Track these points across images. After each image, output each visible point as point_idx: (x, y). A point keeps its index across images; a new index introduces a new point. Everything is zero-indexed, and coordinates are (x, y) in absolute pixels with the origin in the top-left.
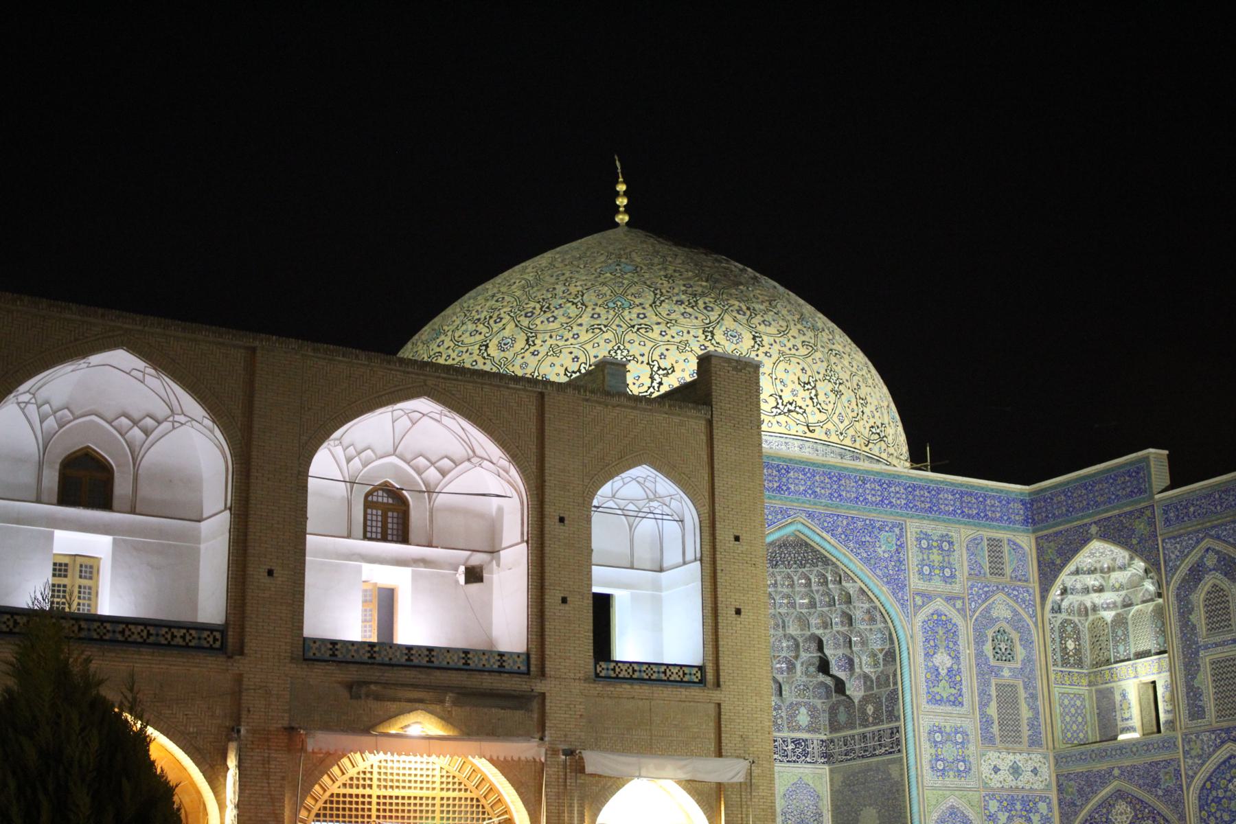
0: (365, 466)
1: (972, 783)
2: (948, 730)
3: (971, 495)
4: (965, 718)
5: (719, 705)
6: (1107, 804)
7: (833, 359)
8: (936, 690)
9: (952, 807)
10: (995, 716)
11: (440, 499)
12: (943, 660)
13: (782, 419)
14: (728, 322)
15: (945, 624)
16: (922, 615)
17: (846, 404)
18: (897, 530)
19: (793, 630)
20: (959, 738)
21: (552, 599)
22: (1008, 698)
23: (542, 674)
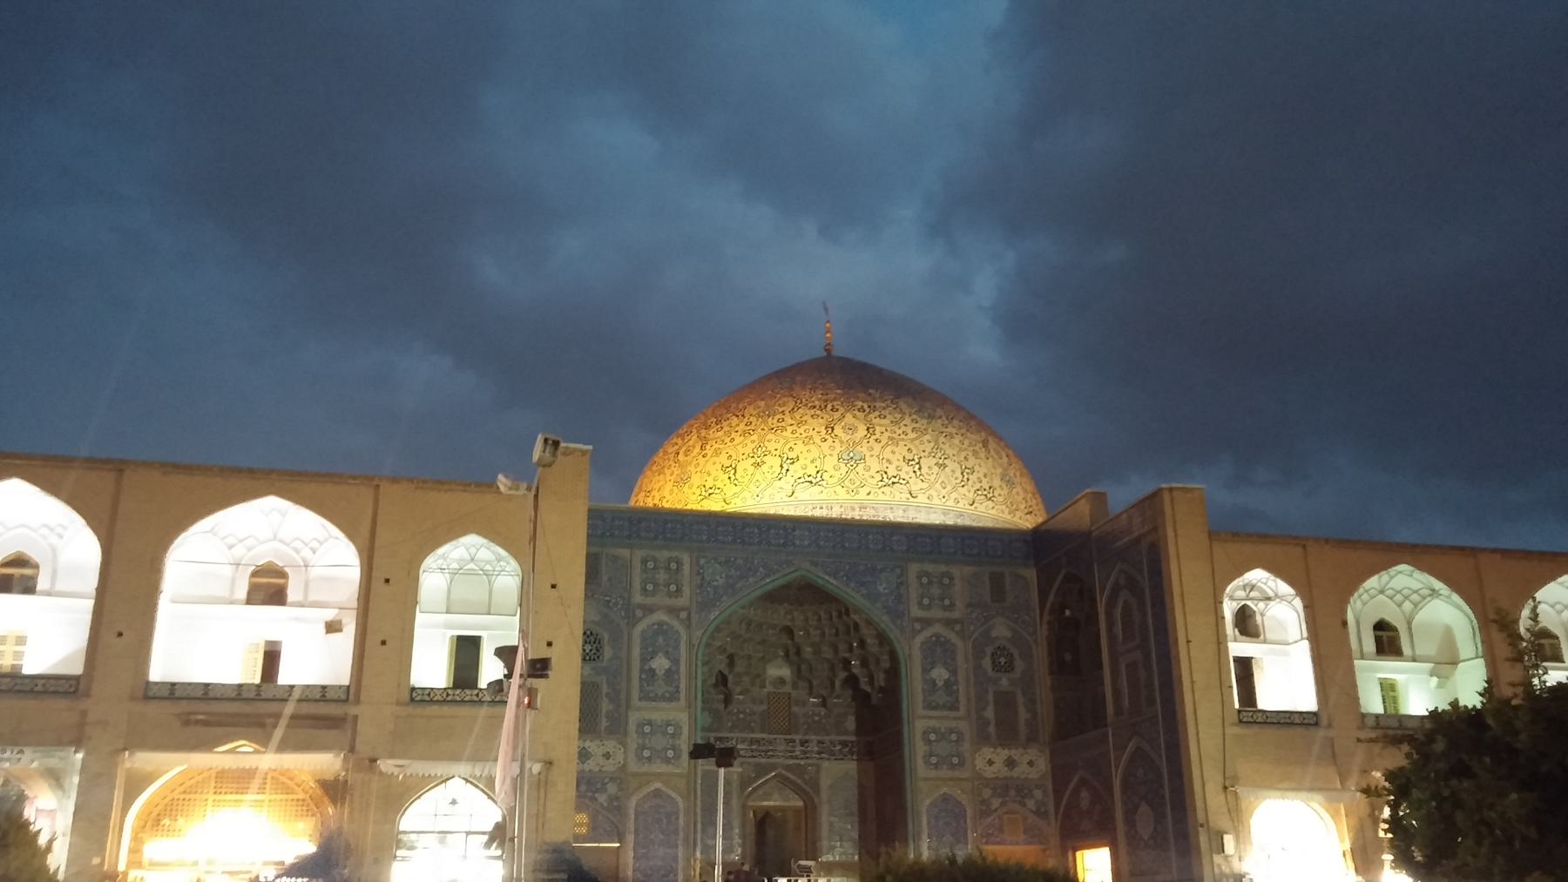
0: (250, 549)
6: (1076, 791)
7: (942, 439)
11: (314, 572)
12: (940, 674)
13: (886, 489)
14: (849, 417)
16: (920, 639)
18: (898, 571)
19: (827, 653)
20: (954, 737)
23: (357, 701)
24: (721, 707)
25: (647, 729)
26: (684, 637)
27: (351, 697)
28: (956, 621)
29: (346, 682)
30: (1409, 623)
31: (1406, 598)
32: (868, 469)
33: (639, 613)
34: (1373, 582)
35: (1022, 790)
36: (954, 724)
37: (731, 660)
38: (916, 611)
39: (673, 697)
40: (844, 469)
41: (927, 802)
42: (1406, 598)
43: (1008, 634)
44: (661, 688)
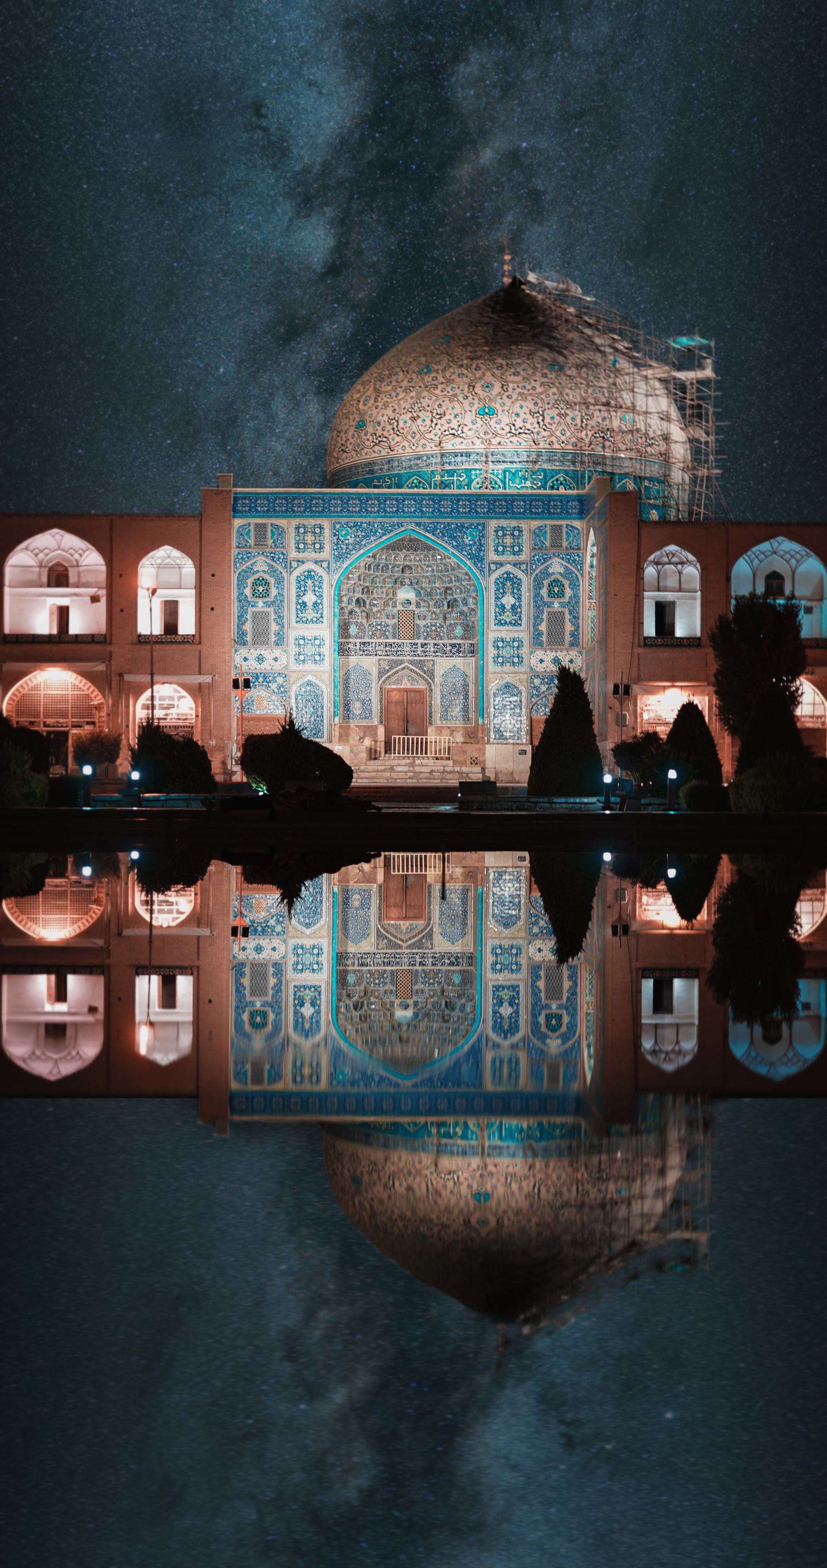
0: (46, 555)
1: (522, 669)
2: (508, 640)
3: (538, 500)
4: (523, 633)
5: (200, 652)
8: (502, 617)
12: (508, 600)
13: (514, 439)
15: (511, 580)
17: (569, 421)
18: (480, 528)
20: (516, 644)
21: (116, 609)
22: (556, 620)
23: (111, 643)
24: (364, 621)
27: (108, 641)
30: (793, 574)
31: (792, 556)
33: (294, 564)
34: (765, 546)
36: (516, 635)
37: (366, 590)
38: (492, 556)
39: (319, 620)
42: (792, 556)
43: (562, 570)
44: (310, 614)
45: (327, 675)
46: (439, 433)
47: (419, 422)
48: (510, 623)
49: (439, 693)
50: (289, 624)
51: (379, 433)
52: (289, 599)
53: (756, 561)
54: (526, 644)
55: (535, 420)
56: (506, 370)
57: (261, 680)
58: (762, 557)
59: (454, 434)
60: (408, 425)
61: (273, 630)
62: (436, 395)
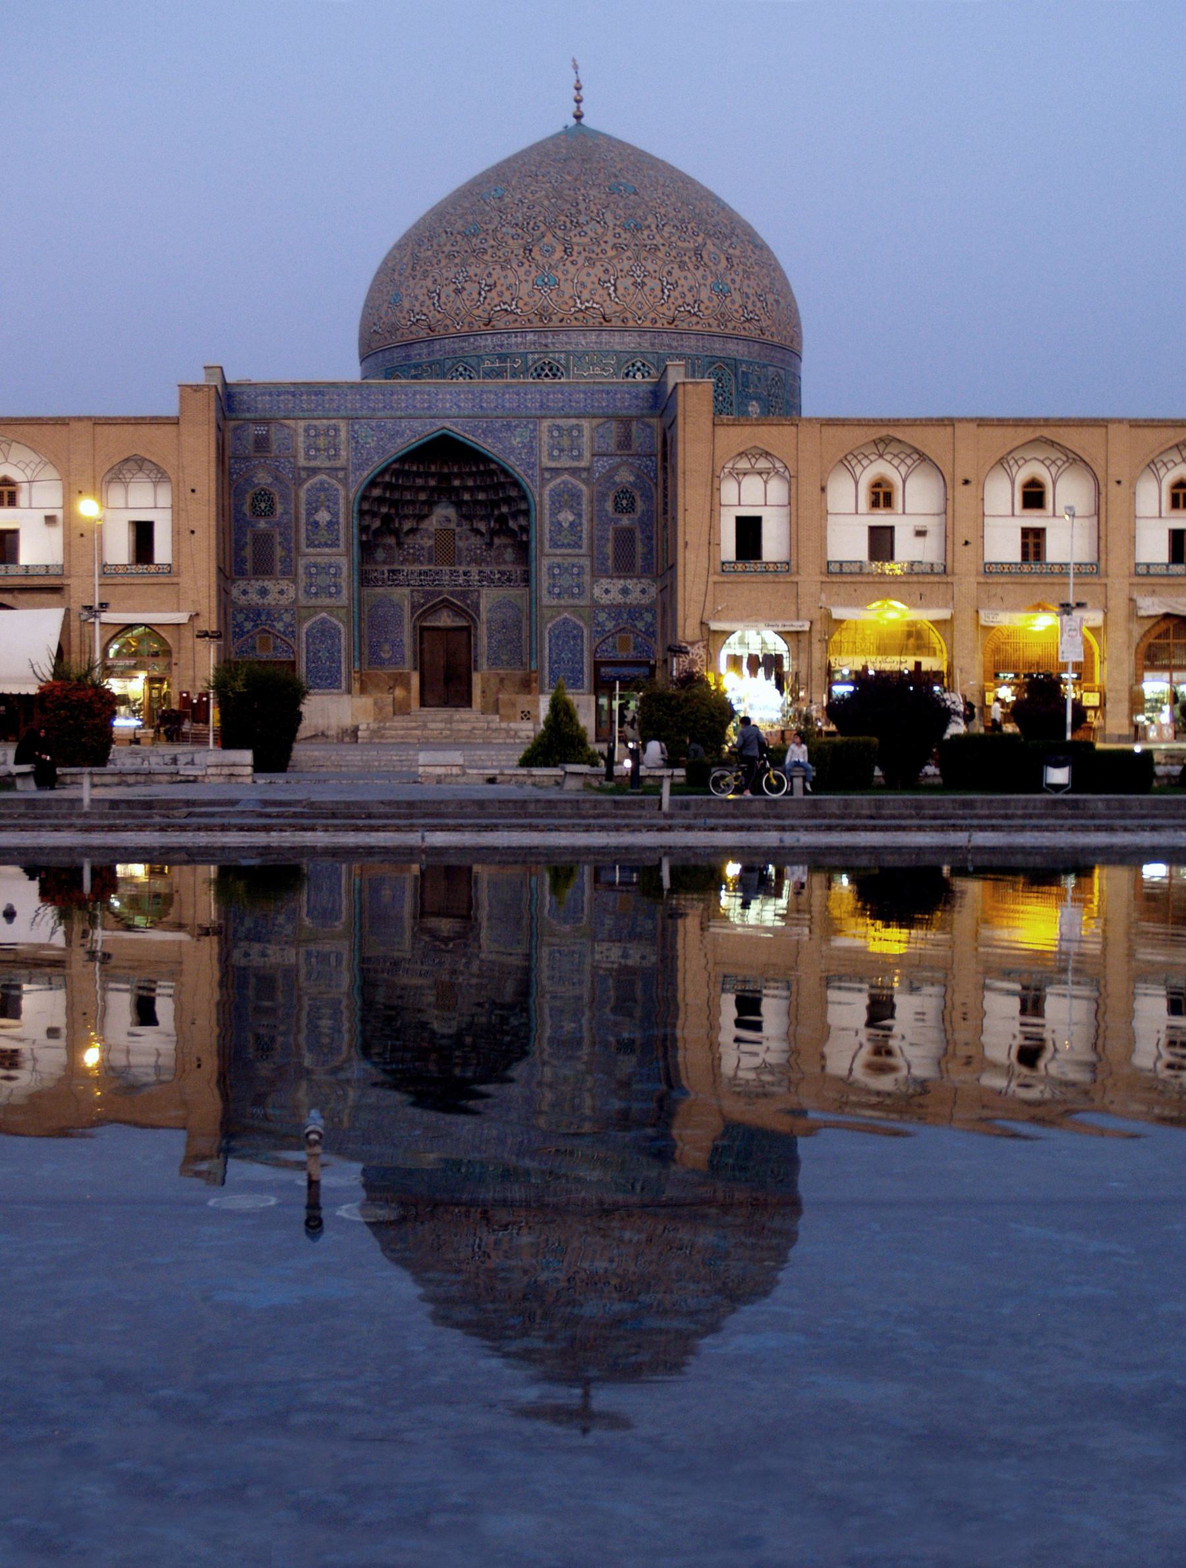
7: (644, 254)
9: (566, 619)
10: (610, 554)
12: (567, 517)
13: (580, 315)
17: (648, 292)
18: (531, 426)
20: (575, 570)
25: (313, 570)
26: (342, 493)
28: (584, 469)
29: (60, 562)
30: (904, 482)
32: (561, 293)
33: (303, 474)
35: (634, 612)
39: (334, 544)
40: (538, 295)
41: (549, 625)
43: (632, 479)
44: (323, 536)
45: (344, 611)
46: (488, 308)
47: (465, 295)
48: (569, 544)
49: (485, 631)
50: (297, 548)
51: (417, 309)
52: (297, 518)
53: (858, 470)
54: (588, 570)
55: (605, 293)
56: (570, 230)
57: (264, 618)
58: (865, 462)
59: (506, 310)
60: (451, 299)
61: (278, 557)
62: (486, 263)
